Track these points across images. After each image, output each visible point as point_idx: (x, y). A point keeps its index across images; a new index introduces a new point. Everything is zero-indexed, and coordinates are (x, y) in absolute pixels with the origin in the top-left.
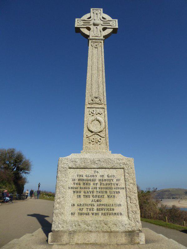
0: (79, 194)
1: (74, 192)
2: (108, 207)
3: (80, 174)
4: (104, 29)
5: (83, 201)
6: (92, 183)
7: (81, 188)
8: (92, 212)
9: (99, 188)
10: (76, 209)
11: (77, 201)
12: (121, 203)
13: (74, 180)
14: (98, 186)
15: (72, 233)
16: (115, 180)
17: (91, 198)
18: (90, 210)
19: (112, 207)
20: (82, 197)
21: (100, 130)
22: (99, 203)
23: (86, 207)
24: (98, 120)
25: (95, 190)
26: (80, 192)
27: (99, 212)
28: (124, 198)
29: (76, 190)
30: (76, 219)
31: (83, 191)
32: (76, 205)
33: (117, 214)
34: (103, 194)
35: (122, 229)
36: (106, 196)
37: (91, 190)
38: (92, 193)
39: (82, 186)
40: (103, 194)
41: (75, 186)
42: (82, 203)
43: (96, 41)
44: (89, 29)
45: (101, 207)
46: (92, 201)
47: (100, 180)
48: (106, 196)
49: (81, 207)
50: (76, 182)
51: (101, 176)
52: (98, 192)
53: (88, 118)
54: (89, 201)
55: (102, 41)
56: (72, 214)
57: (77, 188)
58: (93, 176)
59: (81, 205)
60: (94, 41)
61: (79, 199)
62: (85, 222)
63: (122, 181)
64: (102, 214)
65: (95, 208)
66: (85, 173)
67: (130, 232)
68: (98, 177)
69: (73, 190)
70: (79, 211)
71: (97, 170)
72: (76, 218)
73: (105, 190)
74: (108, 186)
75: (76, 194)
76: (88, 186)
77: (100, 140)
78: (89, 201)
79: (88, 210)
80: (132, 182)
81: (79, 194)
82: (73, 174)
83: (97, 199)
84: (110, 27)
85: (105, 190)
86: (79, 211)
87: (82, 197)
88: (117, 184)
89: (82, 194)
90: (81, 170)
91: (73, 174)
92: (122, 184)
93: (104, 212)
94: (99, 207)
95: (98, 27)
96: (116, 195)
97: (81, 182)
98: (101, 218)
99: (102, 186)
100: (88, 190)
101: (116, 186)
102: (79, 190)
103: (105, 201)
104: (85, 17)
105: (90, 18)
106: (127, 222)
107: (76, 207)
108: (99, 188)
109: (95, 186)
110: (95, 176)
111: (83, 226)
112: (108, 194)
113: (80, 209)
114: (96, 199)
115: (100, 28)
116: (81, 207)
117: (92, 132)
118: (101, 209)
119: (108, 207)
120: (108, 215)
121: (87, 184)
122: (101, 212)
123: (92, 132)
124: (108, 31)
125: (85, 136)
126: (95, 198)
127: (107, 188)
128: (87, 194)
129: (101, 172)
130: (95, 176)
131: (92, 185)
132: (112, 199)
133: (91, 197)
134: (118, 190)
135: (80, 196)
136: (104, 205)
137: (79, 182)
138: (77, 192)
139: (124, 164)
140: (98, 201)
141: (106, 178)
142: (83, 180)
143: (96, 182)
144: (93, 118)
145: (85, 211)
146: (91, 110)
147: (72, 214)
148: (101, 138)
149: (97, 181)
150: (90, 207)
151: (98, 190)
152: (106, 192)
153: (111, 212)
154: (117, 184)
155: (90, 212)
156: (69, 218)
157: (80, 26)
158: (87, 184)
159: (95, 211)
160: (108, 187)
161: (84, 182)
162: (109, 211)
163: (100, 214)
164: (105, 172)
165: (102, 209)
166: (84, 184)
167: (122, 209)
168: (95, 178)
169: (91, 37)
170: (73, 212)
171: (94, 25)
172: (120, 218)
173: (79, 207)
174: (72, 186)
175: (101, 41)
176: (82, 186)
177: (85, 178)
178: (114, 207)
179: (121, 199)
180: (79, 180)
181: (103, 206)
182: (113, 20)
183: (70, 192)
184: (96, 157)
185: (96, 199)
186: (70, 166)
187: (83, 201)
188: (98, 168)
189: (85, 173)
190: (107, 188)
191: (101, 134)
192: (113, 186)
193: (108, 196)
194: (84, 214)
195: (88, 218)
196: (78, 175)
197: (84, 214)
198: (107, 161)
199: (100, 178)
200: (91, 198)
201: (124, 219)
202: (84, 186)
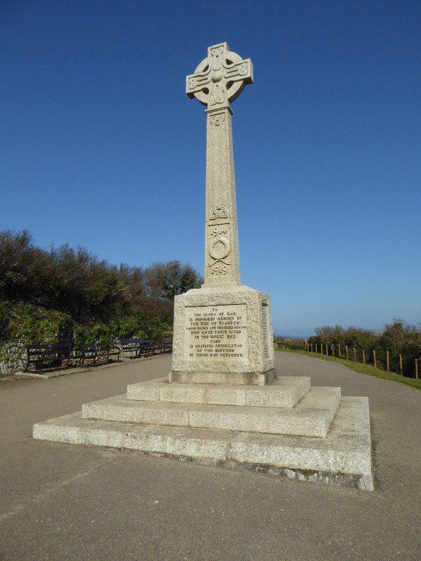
4: (229, 85)
5: (201, 341)
6: (210, 322)
10: (194, 350)
11: (196, 342)
13: (191, 320)
15: (190, 373)
20: (200, 338)
21: (224, 256)
24: (222, 242)
25: (214, 330)
26: (198, 333)
28: (245, 338)
30: (194, 360)
31: (201, 331)
35: (241, 370)
36: (225, 336)
37: (209, 330)
43: (217, 112)
44: (206, 91)
49: (199, 349)
50: (194, 321)
51: (220, 314)
53: (209, 240)
54: (207, 341)
55: (226, 111)
57: (194, 329)
60: (214, 113)
62: (203, 363)
63: (244, 319)
64: (221, 355)
65: (214, 349)
66: (203, 312)
67: (249, 373)
68: (218, 316)
69: (190, 331)
72: (195, 359)
74: (228, 325)
75: (194, 335)
77: (224, 269)
78: (207, 341)
80: (255, 319)
82: (190, 313)
83: (216, 339)
84: (239, 78)
85: (224, 330)
87: (200, 338)
88: (238, 323)
89: (200, 334)
91: (190, 313)
92: (244, 322)
93: (223, 353)
95: (219, 84)
96: (237, 335)
97: (199, 322)
98: (220, 359)
101: (236, 325)
103: (225, 341)
104: (200, 69)
105: (207, 68)
106: (247, 364)
109: (214, 326)
111: (201, 367)
115: (222, 84)
116: (199, 349)
117: (215, 259)
123: (215, 259)
124: (236, 87)
125: (206, 265)
127: (226, 328)
128: (205, 335)
129: (220, 309)
131: (210, 325)
139: (246, 298)
141: (226, 316)
144: (216, 240)
146: (213, 228)
148: (225, 265)
149: (216, 321)
151: (217, 330)
154: (238, 323)
155: (209, 353)
156: (188, 359)
157: (196, 90)
160: (229, 327)
162: (228, 351)
163: (219, 355)
164: (226, 310)
167: (243, 350)
169: (210, 108)
170: (191, 353)
171: (215, 81)
172: (240, 359)
174: (190, 326)
175: (224, 111)
176: (200, 326)
177: (203, 317)
178: (234, 348)
179: (242, 338)
182: (243, 61)
183: (188, 333)
184: (218, 291)
186: (186, 304)
187: (201, 341)
188: (217, 305)
189: (203, 312)
190: (226, 328)
191: (226, 261)
192: (233, 325)
194: (202, 355)
195: (207, 360)
197: (202, 355)
198: (226, 296)
200: (210, 339)
201: (245, 360)
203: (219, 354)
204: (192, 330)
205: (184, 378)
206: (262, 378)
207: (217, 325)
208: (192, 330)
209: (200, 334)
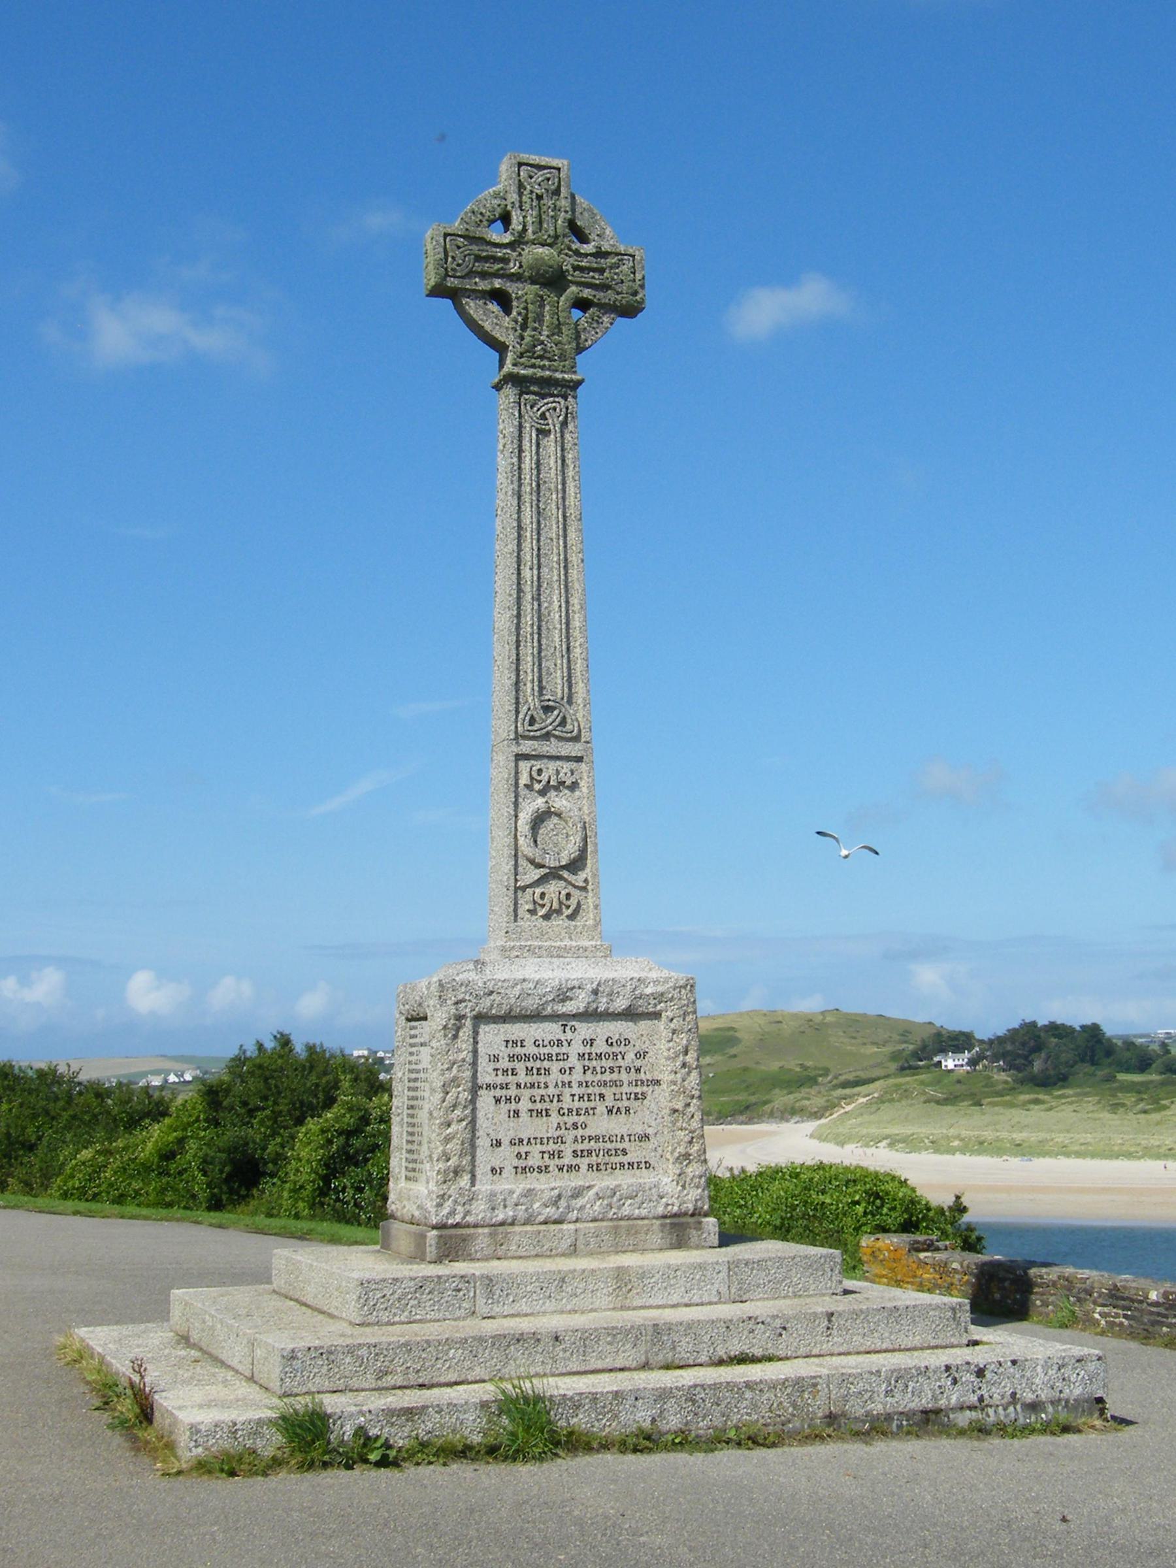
0: (513, 1106)
2: (609, 1145)
3: (514, 1038)
5: (529, 1127)
6: (555, 1067)
7: (518, 1086)
8: (557, 1161)
12: (650, 1131)
13: (496, 1058)
14: (577, 1076)
16: (630, 1056)
17: (555, 1119)
18: (552, 1155)
19: (620, 1146)
20: (524, 1115)
22: (580, 1132)
23: (539, 1147)
25: (567, 1091)
26: (518, 1099)
27: (578, 1161)
29: (504, 1092)
31: (526, 1094)
32: (505, 1142)
33: (635, 1166)
34: (592, 1104)
36: (601, 1108)
37: (551, 1091)
38: (556, 1099)
39: (522, 1078)
40: (592, 1104)
41: (500, 1079)
42: (525, 1137)
45: (585, 1146)
46: (559, 1127)
47: (581, 1056)
49: (523, 1149)
50: (504, 1064)
52: (576, 1098)
54: (545, 1127)
56: (493, 1170)
57: (505, 1086)
59: (521, 1141)
61: (512, 1123)
64: (590, 1166)
65: (568, 1150)
70: (516, 1162)
73: (597, 1090)
74: (607, 1077)
76: (542, 1079)
78: (545, 1127)
79: (546, 1156)
81: (513, 1106)
85: (597, 1090)
86: (516, 1162)
88: (638, 1070)
89: (524, 1105)
93: (593, 1159)
94: (580, 1147)
97: (520, 1067)
99: (589, 1077)
100: (542, 1092)
101: (633, 1076)
102: (513, 1092)
103: (601, 1124)
107: (506, 1151)
108: (580, 1084)
109: (566, 1078)
110: (565, 1043)
112: (609, 1102)
113: (519, 1156)
114: (570, 1120)
116: (523, 1149)
118: (585, 1153)
119: (609, 1145)
120: (609, 1170)
121: (538, 1070)
122: (586, 1161)
126: (565, 1118)
128: (539, 1106)
130: (565, 1043)
131: (555, 1075)
132: (622, 1118)
133: (554, 1114)
134: (639, 1090)
135: (517, 1113)
136: (597, 1139)
137: (511, 1065)
138: (508, 1100)
140: (575, 1126)
141: (600, 1047)
142: (527, 1057)
143: (567, 1065)
145: (534, 1161)
147: (493, 1170)
149: (573, 1060)
150: (551, 1147)
151: (576, 1090)
152: (602, 1096)
153: (614, 1159)
154: (638, 1070)
155: (553, 1163)
158: (538, 1070)
159: (568, 1160)
161: (529, 1065)
163: (584, 1167)
165: (590, 1153)
166: (529, 1071)
168: (564, 1050)
173: (517, 1149)
176: (522, 1078)
177: (531, 1050)
178: (626, 1145)
180: (512, 1058)
181: (592, 1142)
187: (529, 1127)
192: (624, 1076)
193: (610, 1111)
195: (546, 1185)
196: (507, 1041)
199: (582, 1050)
200: (555, 1119)
202: (529, 1079)
203: (584, 1162)
204: (499, 1093)
207: (577, 1076)
208: (499, 1093)
209: (524, 1105)
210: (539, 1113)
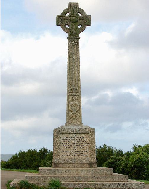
0: (66, 147)
1: (63, 146)
5: (68, 150)
6: (72, 141)
9: (76, 144)
10: (65, 154)
11: (65, 150)
13: (63, 140)
17: (72, 148)
18: (72, 154)
35: (87, 162)
36: (79, 147)
37: (72, 144)
39: (67, 142)
41: (64, 143)
42: (67, 151)
45: (77, 153)
46: (73, 150)
48: (79, 147)
50: (65, 140)
58: (73, 138)
64: (78, 155)
67: (90, 163)
68: (76, 138)
71: (75, 135)
72: (65, 157)
73: (79, 145)
74: (80, 143)
76: (70, 143)
85: (79, 145)
88: (85, 142)
89: (68, 146)
90: (67, 135)
97: (67, 141)
99: (78, 143)
102: (66, 145)
103: (80, 150)
108: (76, 144)
113: (67, 154)
129: (77, 136)
131: (72, 142)
134: (85, 145)
135: (66, 148)
138: (65, 146)
141: (80, 138)
149: (75, 140)
150: (72, 153)
154: (85, 142)
156: (61, 157)
163: (77, 156)
165: (77, 153)
166: (68, 142)
168: (74, 139)
170: (63, 155)
174: (62, 143)
176: (67, 142)
178: (83, 153)
180: (66, 140)
185: (75, 149)
187: (68, 150)
194: (68, 156)
197: (68, 156)
200: (72, 148)
201: (88, 158)
202: (68, 143)
204: (64, 145)
205: (60, 165)
206: (96, 164)
208: (64, 145)
209: (68, 146)
210: (70, 148)
